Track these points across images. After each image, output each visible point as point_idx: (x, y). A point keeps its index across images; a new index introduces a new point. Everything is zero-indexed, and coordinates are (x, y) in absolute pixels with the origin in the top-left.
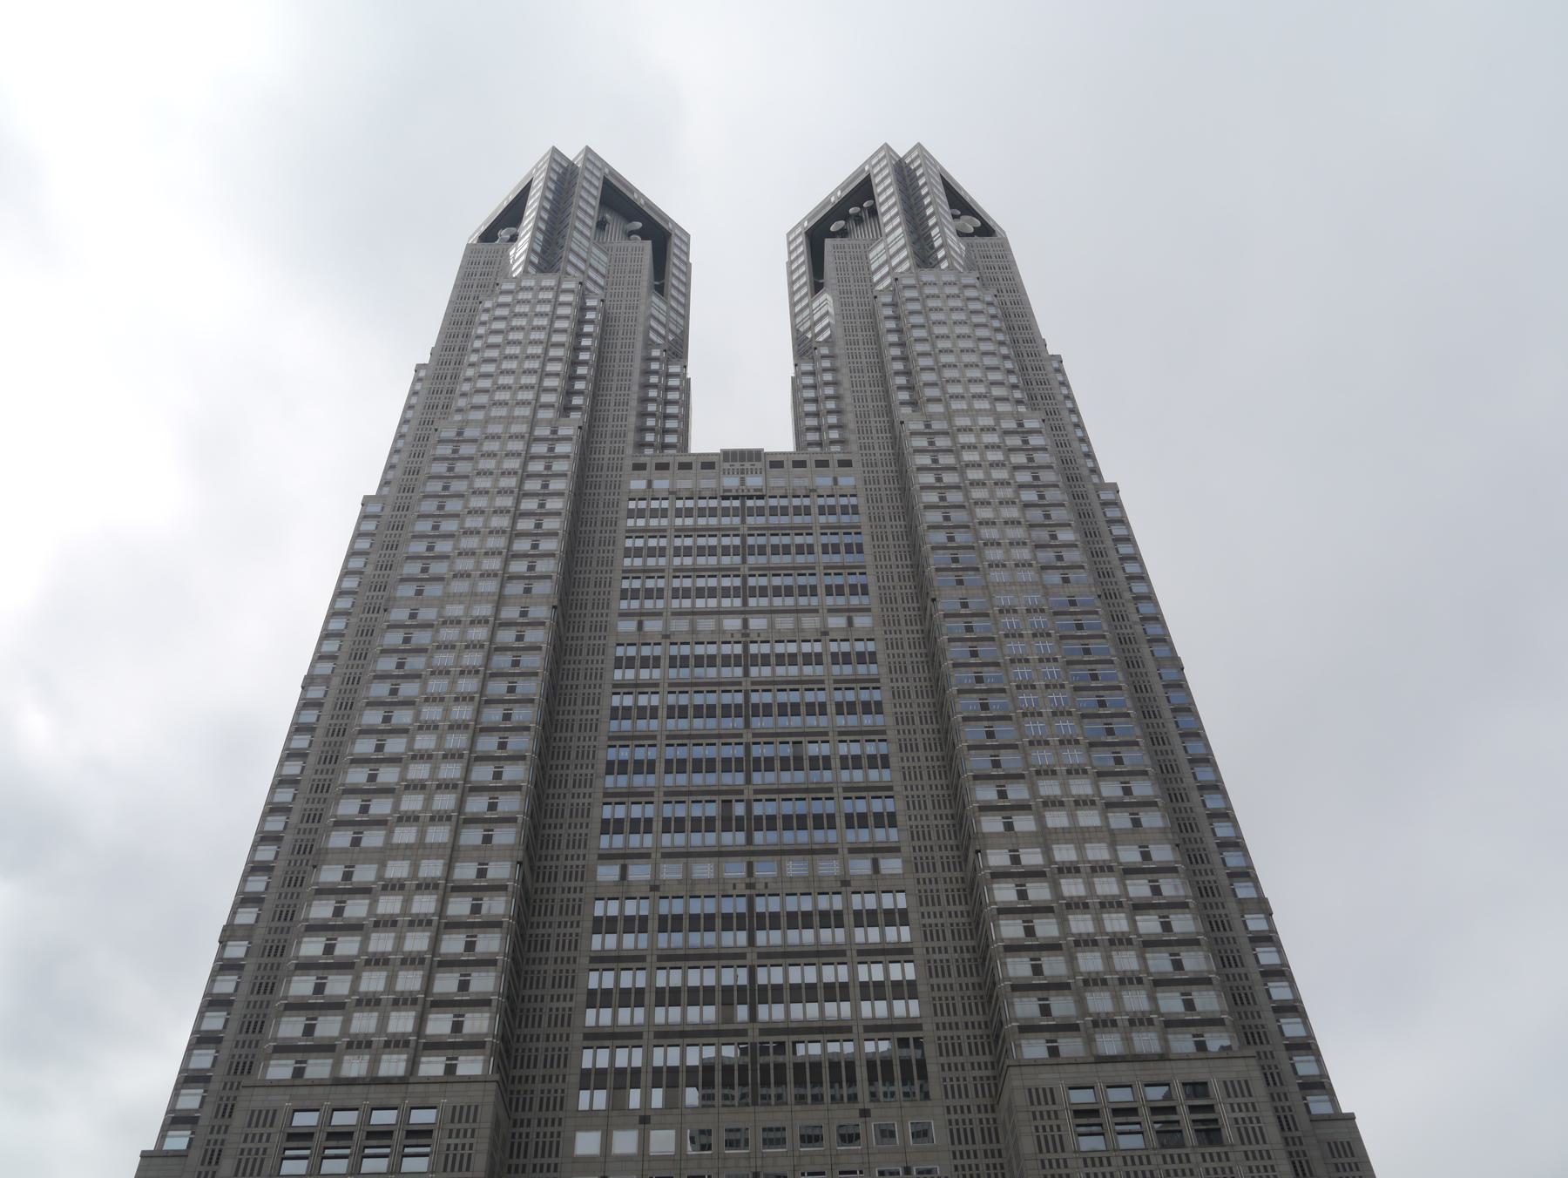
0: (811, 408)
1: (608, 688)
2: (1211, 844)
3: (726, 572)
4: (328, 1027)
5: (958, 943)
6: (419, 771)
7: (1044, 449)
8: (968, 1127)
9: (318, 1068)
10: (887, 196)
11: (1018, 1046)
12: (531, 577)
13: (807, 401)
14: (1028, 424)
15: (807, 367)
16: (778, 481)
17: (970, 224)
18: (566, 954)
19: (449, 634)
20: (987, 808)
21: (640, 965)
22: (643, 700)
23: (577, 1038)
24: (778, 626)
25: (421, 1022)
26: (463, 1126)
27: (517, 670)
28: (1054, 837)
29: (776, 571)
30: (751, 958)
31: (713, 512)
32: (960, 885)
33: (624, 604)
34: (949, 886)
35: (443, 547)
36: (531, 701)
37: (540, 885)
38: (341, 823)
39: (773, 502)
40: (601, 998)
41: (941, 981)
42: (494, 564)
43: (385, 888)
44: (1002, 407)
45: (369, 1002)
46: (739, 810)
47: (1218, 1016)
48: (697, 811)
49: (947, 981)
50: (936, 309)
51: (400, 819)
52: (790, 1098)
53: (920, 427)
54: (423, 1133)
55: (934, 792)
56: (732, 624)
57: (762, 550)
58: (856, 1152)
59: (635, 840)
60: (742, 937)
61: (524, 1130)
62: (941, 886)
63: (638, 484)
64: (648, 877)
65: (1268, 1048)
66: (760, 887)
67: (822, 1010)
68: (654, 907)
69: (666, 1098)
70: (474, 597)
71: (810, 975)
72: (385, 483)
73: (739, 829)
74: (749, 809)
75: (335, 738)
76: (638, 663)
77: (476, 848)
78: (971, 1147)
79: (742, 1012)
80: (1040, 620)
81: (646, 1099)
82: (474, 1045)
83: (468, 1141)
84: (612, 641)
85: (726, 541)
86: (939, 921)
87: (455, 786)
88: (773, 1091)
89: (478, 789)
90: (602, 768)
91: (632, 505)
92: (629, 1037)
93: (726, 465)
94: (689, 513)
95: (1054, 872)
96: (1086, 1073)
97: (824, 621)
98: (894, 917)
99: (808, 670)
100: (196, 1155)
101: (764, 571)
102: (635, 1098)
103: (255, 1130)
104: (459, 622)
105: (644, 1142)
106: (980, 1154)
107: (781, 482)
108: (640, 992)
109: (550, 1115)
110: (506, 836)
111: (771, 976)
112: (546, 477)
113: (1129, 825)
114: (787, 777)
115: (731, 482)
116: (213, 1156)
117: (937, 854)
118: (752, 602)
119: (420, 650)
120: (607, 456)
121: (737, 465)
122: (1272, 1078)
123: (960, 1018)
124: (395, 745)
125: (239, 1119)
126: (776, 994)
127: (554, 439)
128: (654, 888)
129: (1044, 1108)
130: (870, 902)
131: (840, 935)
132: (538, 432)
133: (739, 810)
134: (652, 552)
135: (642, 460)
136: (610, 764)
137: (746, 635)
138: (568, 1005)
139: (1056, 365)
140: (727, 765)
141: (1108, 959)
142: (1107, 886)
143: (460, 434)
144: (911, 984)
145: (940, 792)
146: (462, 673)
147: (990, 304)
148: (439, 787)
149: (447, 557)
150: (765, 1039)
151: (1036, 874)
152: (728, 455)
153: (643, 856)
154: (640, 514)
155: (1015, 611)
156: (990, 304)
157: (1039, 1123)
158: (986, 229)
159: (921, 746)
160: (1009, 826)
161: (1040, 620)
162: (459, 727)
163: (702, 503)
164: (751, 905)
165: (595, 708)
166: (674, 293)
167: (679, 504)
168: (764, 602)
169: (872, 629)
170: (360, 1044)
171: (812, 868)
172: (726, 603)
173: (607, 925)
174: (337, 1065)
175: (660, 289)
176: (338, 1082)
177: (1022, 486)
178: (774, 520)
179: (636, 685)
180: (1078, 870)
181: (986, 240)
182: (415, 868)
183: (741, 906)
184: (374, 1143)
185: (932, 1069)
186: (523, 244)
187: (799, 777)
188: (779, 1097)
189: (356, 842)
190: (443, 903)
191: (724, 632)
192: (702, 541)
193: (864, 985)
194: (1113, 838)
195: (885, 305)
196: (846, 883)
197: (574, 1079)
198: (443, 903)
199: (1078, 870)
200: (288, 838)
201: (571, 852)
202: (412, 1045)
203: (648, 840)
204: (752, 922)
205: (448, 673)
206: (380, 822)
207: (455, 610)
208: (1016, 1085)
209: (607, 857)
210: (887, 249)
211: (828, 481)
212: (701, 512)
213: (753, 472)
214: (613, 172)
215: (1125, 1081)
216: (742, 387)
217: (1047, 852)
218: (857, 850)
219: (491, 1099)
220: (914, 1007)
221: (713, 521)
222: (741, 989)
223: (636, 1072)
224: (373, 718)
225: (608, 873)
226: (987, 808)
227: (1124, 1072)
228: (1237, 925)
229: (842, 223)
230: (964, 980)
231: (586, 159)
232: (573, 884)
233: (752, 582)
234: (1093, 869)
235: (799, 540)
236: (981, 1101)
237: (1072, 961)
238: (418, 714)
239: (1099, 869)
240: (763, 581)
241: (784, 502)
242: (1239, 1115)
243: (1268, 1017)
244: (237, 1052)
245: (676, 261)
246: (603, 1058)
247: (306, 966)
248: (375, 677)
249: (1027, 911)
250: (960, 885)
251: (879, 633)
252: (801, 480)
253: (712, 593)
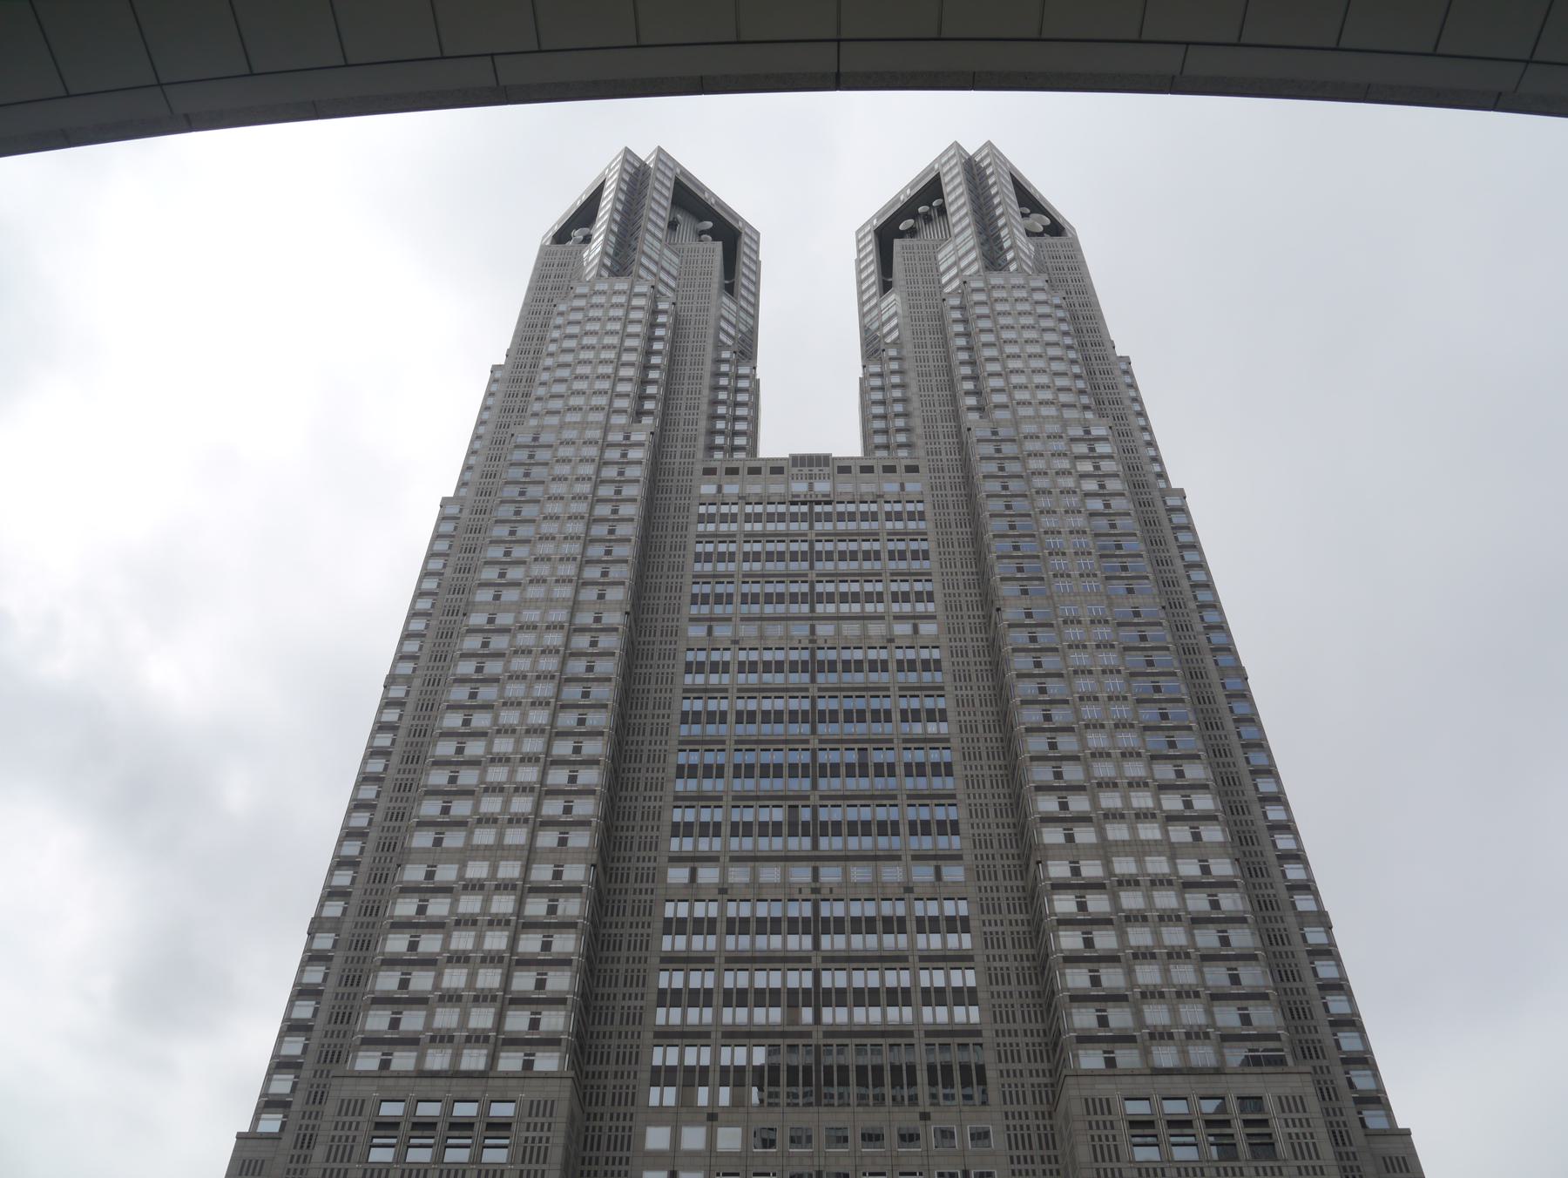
0: (879, 410)
1: (679, 693)
2: (1271, 857)
3: (794, 578)
4: (413, 1021)
5: (1018, 952)
6: (497, 774)
7: (1110, 457)
8: (1025, 1132)
9: (403, 1061)
10: (956, 196)
11: (1076, 1056)
12: (604, 583)
13: (875, 403)
14: (1095, 432)
15: (876, 369)
16: (846, 486)
17: (1038, 222)
18: (637, 954)
19: (526, 639)
20: (1048, 819)
21: (708, 966)
22: (712, 705)
23: (648, 1036)
24: (845, 633)
25: (500, 1018)
26: (540, 1120)
27: (591, 676)
28: (1114, 849)
29: (843, 577)
30: (816, 962)
31: (781, 518)
32: (1021, 894)
33: (694, 610)
34: (1010, 894)
35: (519, 552)
36: (605, 706)
37: (612, 886)
38: (424, 824)
39: (841, 508)
40: (672, 998)
41: (1001, 988)
42: (569, 570)
43: (465, 887)
44: (1069, 414)
45: (451, 998)
46: (805, 815)
47: (1274, 1031)
48: (764, 815)
49: (1007, 988)
50: (1008, 327)
51: (479, 821)
52: (853, 1100)
53: (988, 434)
54: (501, 1126)
55: (996, 800)
56: (800, 631)
57: (829, 556)
58: (916, 1155)
59: (704, 844)
60: (807, 941)
61: (598, 1123)
62: (1003, 895)
63: (708, 489)
64: (716, 880)
65: (1325, 1063)
66: (825, 891)
67: (884, 1015)
68: (722, 909)
69: (733, 1097)
70: (550, 602)
71: (873, 979)
72: (462, 484)
73: (805, 834)
74: (815, 814)
75: (417, 739)
76: (707, 668)
77: (552, 850)
78: (1028, 1153)
79: (807, 1014)
80: (1104, 632)
81: (714, 1096)
82: (551, 1042)
83: (545, 1134)
84: (682, 646)
85: (794, 547)
86: (1000, 929)
87: (532, 789)
88: (835, 1090)
89: (555, 792)
90: (672, 771)
91: (702, 509)
92: (696, 1036)
93: (795, 470)
94: (758, 518)
95: (1113, 885)
96: (1143, 1085)
97: (890, 628)
98: (956, 924)
99: (874, 677)
100: (288, 1139)
101: (832, 577)
102: (703, 1096)
103: (345, 1119)
104: (535, 627)
105: (711, 1139)
106: (1037, 1159)
107: (849, 488)
108: (708, 992)
109: (622, 1109)
110: (581, 839)
111: (834, 979)
112: (619, 483)
113: (1189, 839)
114: (853, 784)
115: (800, 487)
116: (306, 1141)
117: (998, 862)
118: (820, 608)
119: (498, 655)
120: (678, 460)
121: (806, 470)
122: (1326, 1093)
123: (1019, 1026)
124: (475, 748)
125: (330, 1108)
126: (839, 997)
127: (627, 444)
128: (723, 891)
129: (1099, 1118)
130: (933, 909)
131: (903, 940)
132: (612, 437)
133: (805, 815)
134: (721, 557)
135: (713, 464)
136: (680, 768)
137: (812, 641)
138: (639, 1003)
139: (1124, 366)
140: (793, 770)
141: (1166, 972)
142: (1166, 900)
143: (535, 439)
144: (972, 991)
145: (1002, 801)
146: (538, 677)
147: (1058, 307)
148: (516, 790)
149: (524, 563)
150: (829, 1041)
151: (1096, 886)
152: (799, 461)
153: (711, 859)
154: (711, 518)
155: (1079, 622)
156: (1058, 307)
157: (1095, 1132)
158: (1056, 228)
159: (984, 755)
160: (1070, 838)
161: (1104, 632)
162: (535, 731)
163: (771, 509)
164: (816, 909)
165: (667, 711)
166: (744, 292)
167: (749, 509)
168: (831, 608)
169: (937, 637)
170: (442, 1039)
171: (876, 873)
172: (794, 609)
173: (676, 926)
174: (421, 1058)
175: (730, 289)
176: (422, 1074)
177: (1088, 495)
178: (841, 526)
179: (706, 690)
180: (1137, 883)
181: (1056, 239)
182: (494, 869)
183: (807, 910)
184: (456, 1133)
185: (991, 1074)
186: (596, 246)
187: (864, 783)
188: (841, 1096)
189: (438, 842)
190: (521, 903)
191: (792, 638)
192: (770, 547)
193: (926, 991)
194: (1175, 853)
195: (953, 308)
196: (909, 890)
197: (645, 1076)
198: (521, 903)
199: (1137, 883)
200: (374, 835)
201: (642, 854)
202: (492, 1040)
203: (717, 844)
204: (816, 926)
205: (525, 677)
206: (460, 824)
207: (531, 616)
208: (1074, 1093)
209: (678, 859)
210: (956, 250)
211: (895, 487)
212: (771, 518)
213: (822, 477)
214: (684, 173)
215: (1180, 1093)
216: (810, 390)
217: (1107, 864)
218: (919, 857)
219: (567, 1094)
220: (974, 1014)
221: (782, 527)
222: (806, 991)
223: (704, 1070)
224: (453, 721)
225: (678, 875)
226: (1048, 819)
227: (1179, 1084)
228: (1296, 939)
229: (911, 222)
230: (1023, 988)
231: (658, 159)
232: (644, 886)
233: (819, 588)
234: (1153, 883)
235: (866, 546)
236: (1039, 1108)
237: (1130, 973)
238: (496, 719)
239: (1158, 882)
240: (830, 588)
241: (851, 508)
242: (1293, 1130)
243: (1325, 1031)
244: (326, 1041)
245: (746, 260)
246: (672, 1057)
247: (392, 962)
248: (456, 681)
249: (1085, 922)
250: (1021, 894)
251: (944, 641)
252: (867, 486)
253: (780, 598)
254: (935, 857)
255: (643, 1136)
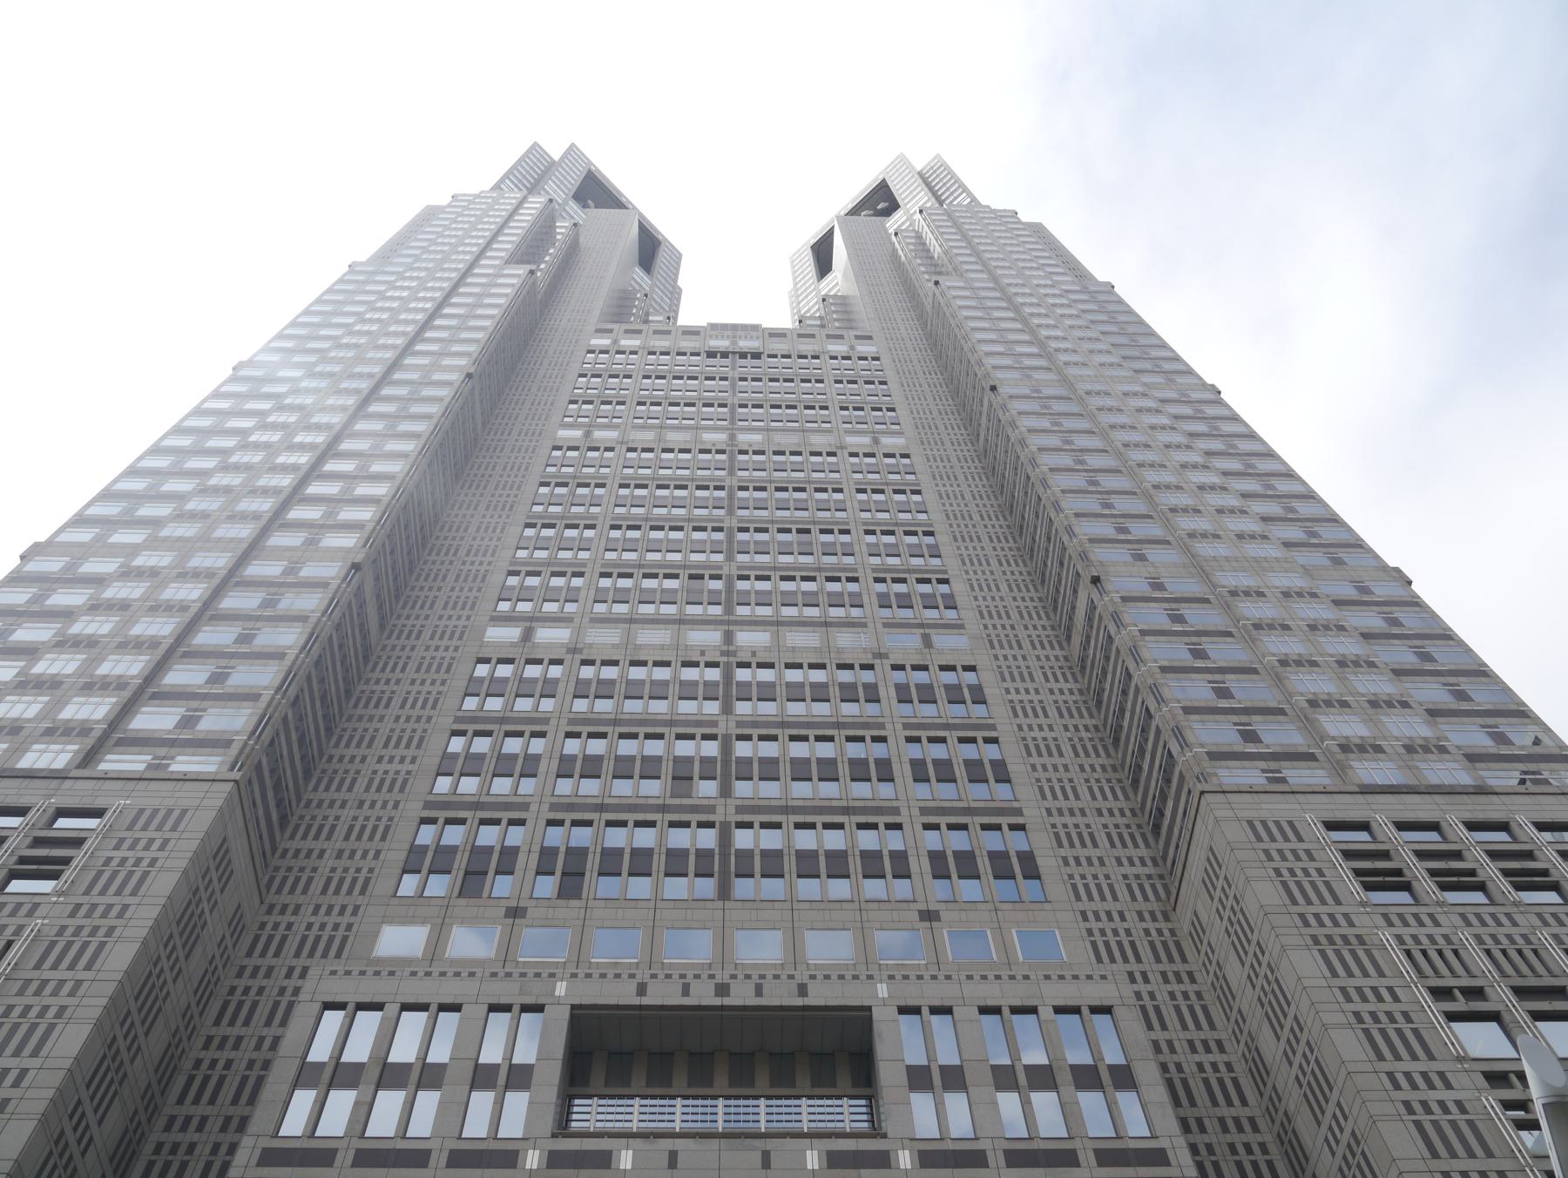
128: (573, 650)
254: (921, 626)
255: (375, 935)
